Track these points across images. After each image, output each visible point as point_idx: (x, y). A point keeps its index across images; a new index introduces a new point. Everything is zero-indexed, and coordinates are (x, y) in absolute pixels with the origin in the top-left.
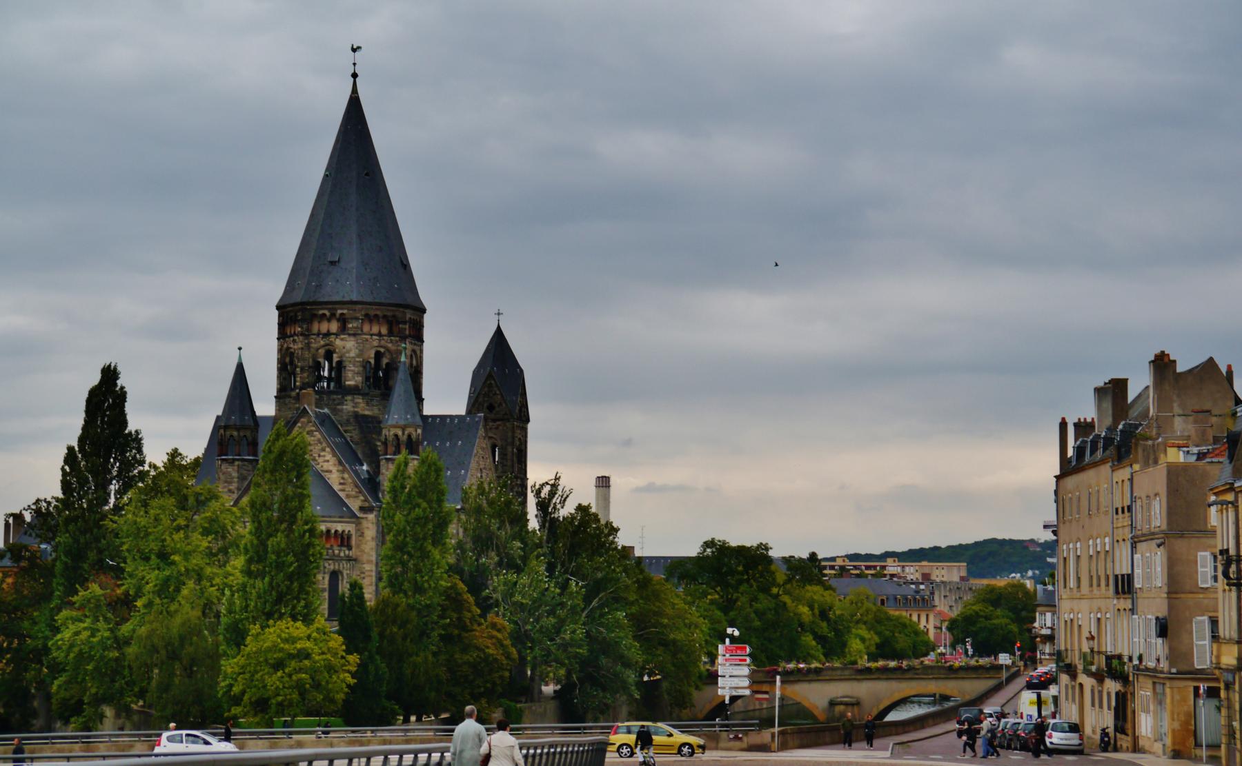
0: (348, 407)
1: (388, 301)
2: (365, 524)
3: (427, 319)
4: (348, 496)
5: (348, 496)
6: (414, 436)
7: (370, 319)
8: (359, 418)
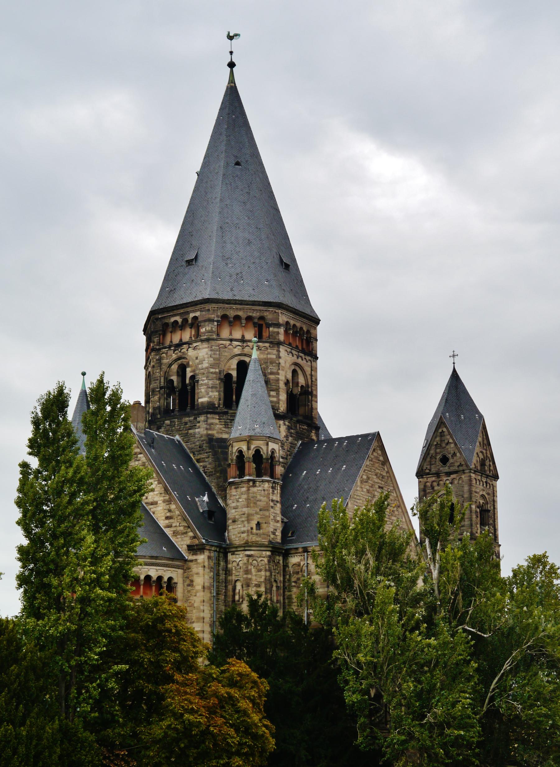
0: (201, 430)
1: (252, 299)
2: (196, 569)
3: (321, 331)
4: (175, 533)
5: (175, 533)
6: (265, 451)
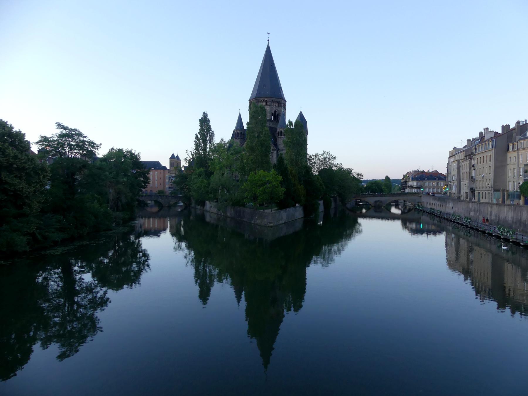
7: (273, 102)
8: (271, 128)
